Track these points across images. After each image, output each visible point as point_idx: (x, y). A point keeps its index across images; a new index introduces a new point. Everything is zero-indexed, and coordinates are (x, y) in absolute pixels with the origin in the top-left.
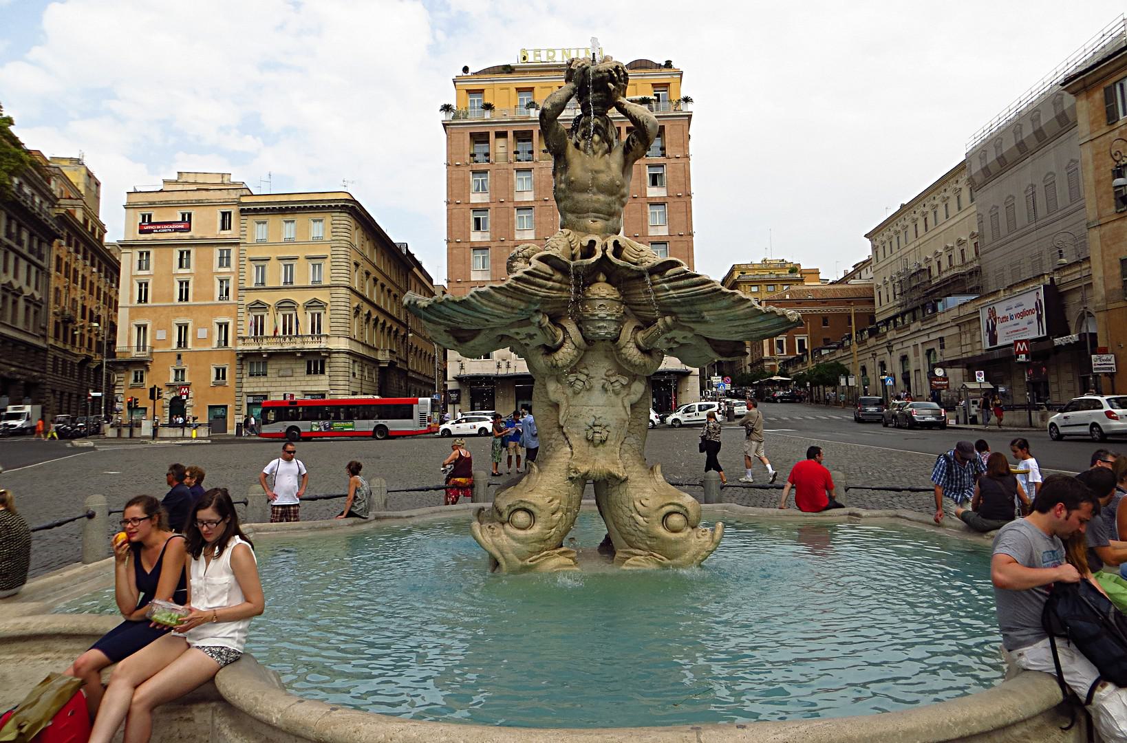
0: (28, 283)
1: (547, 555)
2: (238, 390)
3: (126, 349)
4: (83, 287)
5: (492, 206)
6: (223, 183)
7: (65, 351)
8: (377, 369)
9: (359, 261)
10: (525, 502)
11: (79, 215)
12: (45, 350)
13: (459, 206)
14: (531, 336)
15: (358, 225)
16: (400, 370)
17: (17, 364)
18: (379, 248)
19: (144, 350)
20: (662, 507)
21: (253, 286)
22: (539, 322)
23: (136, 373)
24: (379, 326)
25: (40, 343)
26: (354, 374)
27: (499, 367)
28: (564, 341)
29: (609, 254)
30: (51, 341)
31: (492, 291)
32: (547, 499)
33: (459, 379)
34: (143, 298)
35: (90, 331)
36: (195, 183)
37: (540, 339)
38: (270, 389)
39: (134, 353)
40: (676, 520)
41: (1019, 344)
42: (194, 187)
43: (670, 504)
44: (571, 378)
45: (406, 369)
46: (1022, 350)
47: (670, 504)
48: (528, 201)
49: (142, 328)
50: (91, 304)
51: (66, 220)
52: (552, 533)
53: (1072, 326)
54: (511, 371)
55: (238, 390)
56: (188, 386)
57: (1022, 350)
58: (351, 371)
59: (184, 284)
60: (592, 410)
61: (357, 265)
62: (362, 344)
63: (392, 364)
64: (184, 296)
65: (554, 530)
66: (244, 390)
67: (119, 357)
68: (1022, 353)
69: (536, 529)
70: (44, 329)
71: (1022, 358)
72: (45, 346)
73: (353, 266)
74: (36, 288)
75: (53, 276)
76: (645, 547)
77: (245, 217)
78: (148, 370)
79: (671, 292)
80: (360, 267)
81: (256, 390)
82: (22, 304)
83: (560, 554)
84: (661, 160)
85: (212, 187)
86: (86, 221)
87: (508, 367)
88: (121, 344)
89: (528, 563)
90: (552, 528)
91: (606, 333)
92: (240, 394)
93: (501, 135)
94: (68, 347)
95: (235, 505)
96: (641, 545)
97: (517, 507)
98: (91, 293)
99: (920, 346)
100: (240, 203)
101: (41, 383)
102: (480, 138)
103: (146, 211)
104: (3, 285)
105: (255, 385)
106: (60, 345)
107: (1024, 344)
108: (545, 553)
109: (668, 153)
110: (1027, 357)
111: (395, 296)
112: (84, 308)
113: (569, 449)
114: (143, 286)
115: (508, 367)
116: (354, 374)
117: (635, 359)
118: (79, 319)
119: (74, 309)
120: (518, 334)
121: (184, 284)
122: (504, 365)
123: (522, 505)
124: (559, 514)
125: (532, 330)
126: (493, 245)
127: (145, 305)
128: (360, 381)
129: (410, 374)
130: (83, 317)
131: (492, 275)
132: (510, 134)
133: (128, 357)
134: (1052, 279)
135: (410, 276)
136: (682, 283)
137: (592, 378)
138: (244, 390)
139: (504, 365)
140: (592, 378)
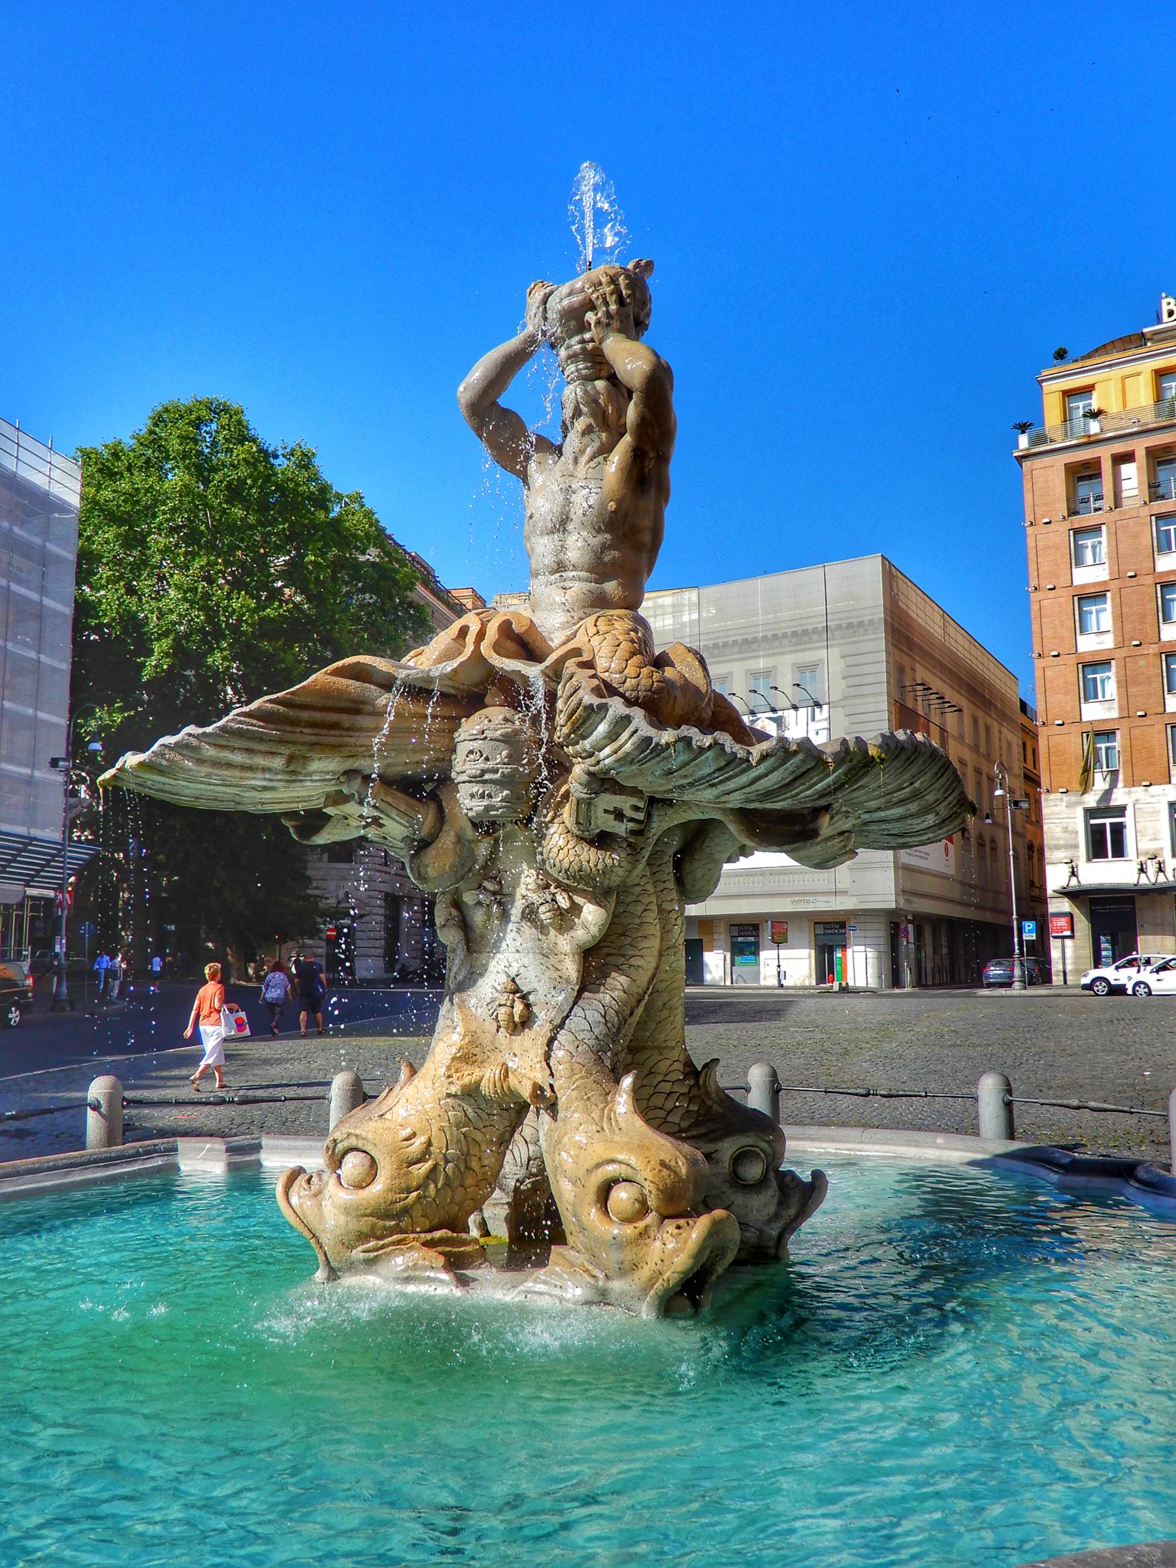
1: (399, 1242)
13: (1052, 594)
20: (598, 1165)
27: (1142, 870)
29: (486, 648)
33: (1067, 893)
40: (622, 1196)
43: (613, 1161)
47: (613, 1161)
69: (378, 1188)
83: (426, 1244)
87: (1161, 870)
90: (409, 1191)
91: (488, 808)
115: (1161, 870)
122: (1152, 867)
131: (1121, 708)
132: (1141, 454)
139: (1152, 867)
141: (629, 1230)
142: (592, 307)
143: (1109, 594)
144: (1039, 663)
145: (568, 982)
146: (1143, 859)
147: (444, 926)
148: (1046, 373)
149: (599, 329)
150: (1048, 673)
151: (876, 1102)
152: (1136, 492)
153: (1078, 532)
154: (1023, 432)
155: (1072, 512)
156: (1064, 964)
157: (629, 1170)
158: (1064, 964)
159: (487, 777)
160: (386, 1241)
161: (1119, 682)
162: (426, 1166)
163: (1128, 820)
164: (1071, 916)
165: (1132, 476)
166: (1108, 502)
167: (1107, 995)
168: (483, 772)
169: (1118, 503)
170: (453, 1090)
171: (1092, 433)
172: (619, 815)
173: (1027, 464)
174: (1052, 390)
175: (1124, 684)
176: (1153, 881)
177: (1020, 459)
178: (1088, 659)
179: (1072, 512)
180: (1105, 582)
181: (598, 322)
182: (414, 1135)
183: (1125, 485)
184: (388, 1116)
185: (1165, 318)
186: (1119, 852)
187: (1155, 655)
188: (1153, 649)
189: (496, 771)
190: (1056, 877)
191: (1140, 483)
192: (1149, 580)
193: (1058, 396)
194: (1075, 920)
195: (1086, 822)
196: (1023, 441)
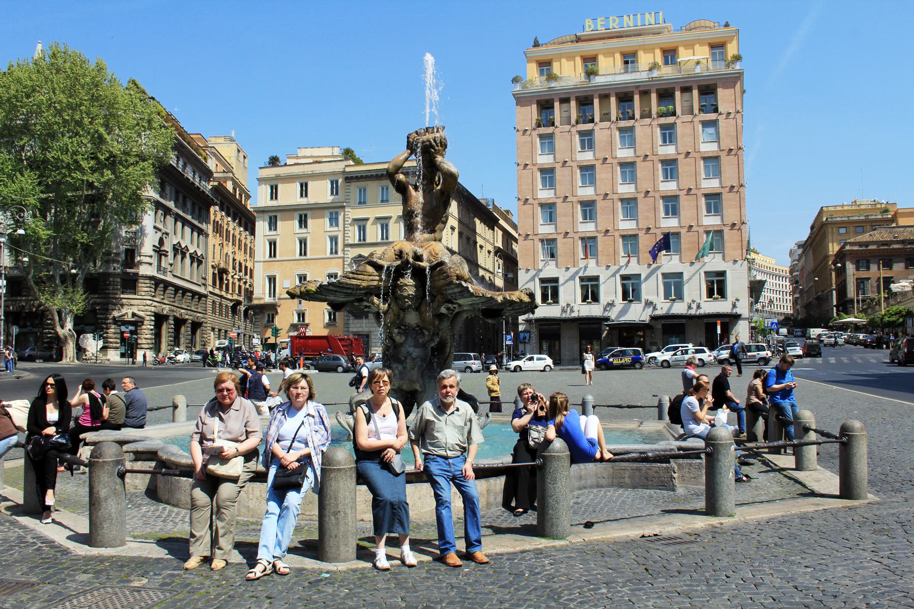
0: (192, 242)
2: (346, 329)
3: (262, 296)
4: (234, 244)
6: (333, 156)
7: (221, 297)
11: (229, 186)
12: (206, 296)
14: (369, 307)
17: (186, 307)
19: (274, 296)
21: (357, 242)
23: (269, 315)
25: (201, 290)
30: (210, 289)
34: (273, 253)
35: (240, 280)
36: (311, 157)
38: (371, 329)
39: (268, 300)
42: (311, 160)
49: (272, 280)
50: (240, 257)
51: (219, 190)
55: (346, 329)
56: (307, 325)
59: (303, 242)
64: (303, 252)
66: (351, 330)
67: (255, 302)
70: (205, 279)
72: (206, 293)
74: (198, 246)
75: (210, 236)
77: (349, 184)
78: (277, 313)
81: (360, 330)
82: (188, 260)
84: (713, 116)
85: (324, 160)
86: (235, 189)
88: (257, 293)
92: (347, 333)
94: (224, 293)
98: (240, 248)
100: (344, 172)
101: (202, 322)
102: (545, 105)
103: (274, 183)
104: (174, 245)
105: (359, 325)
106: (217, 291)
109: (720, 110)
112: (234, 260)
114: (273, 244)
115: (572, 311)
118: (231, 270)
119: (226, 262)
121: (303, 242)
127: (274, 259)
130: (234, 268)
133: (262, 302)
138: (351, 330)
155: (539, 126)
172: (448, 309)
178: (543, 201)
179: (539, 125)
185: (587, 29)
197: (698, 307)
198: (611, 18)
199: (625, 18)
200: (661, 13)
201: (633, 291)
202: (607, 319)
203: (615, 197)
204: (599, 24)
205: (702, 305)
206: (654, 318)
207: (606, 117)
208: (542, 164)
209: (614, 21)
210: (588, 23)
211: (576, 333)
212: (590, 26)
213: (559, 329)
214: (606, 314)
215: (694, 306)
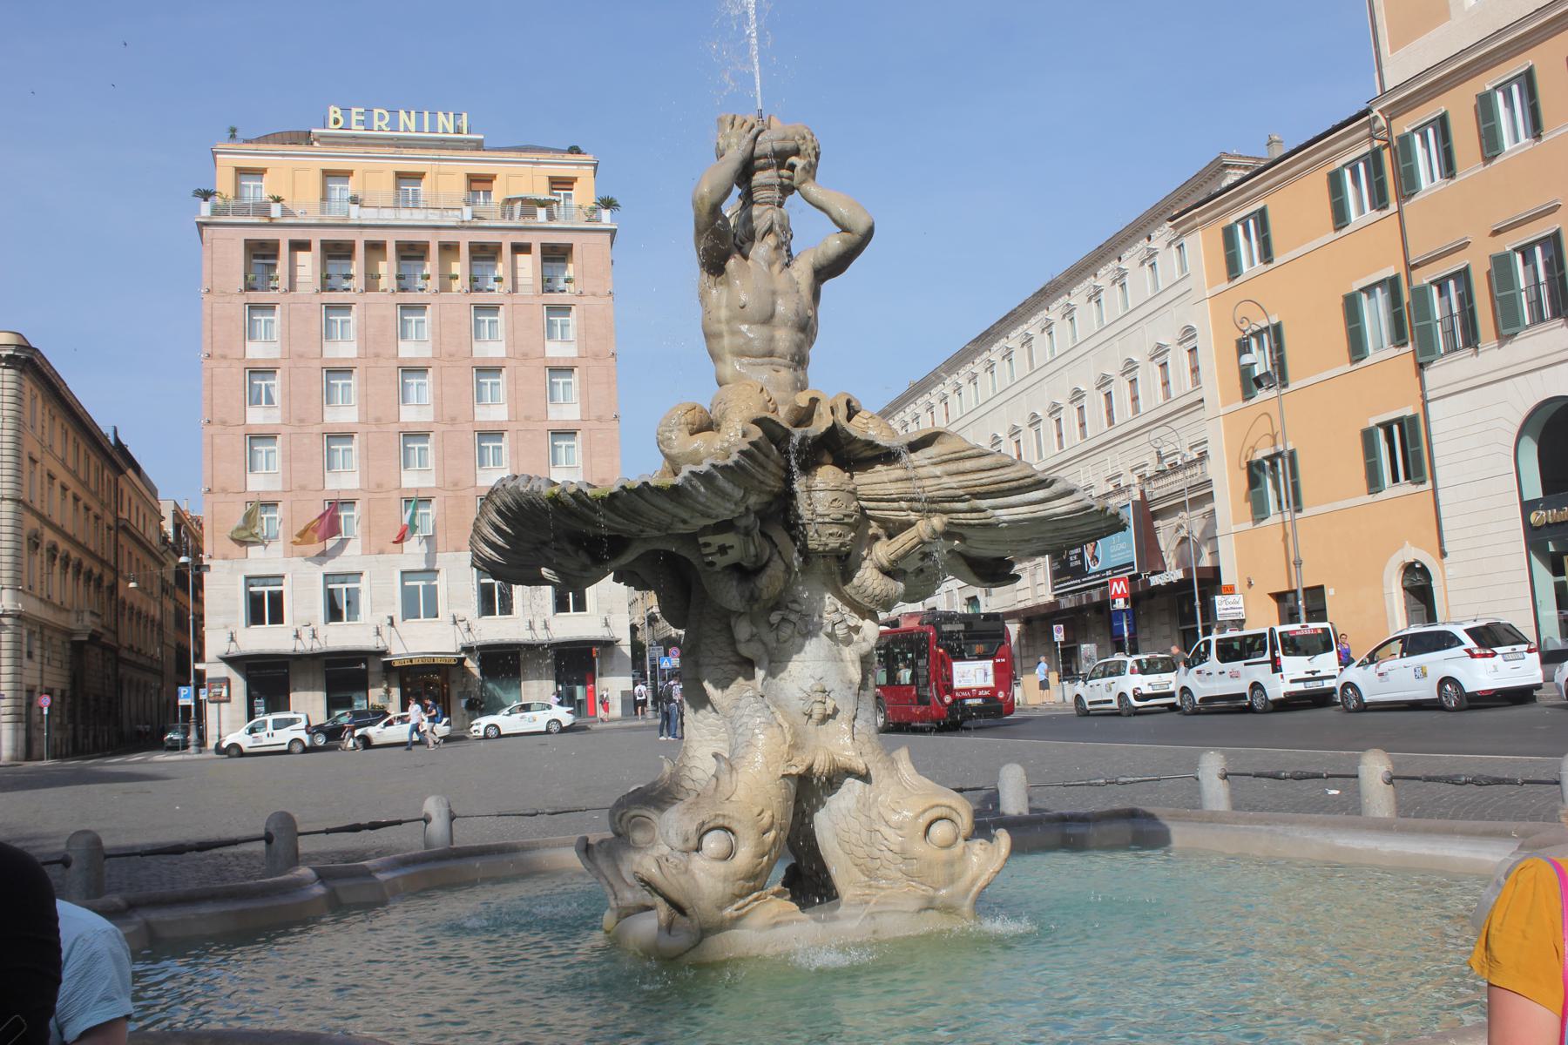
1: (756, 899)
5: (284, 364)
8: (68, 646)
9: (37, 455)
10: (724, 816)
14: (723, 550)
15: (36, 391)
16: (105, 647)
18: (71, 434)
20: (925, 811)
22: (746, 527)
24: (70, 570)
26: (30, 655)
27: (297, 636)
28: (769, 560)
31: (713, 470)
32: (757, 810)
37: (732, 557)
41: (1115, 584)
43: (937, 806)
44: (775, 618)
45: (115, 644)
46: (1119, 592)
48: (346, 359)
52: (763, 864)
53: (1170, 560)
54: (317, 646)
57: (1119, 592)
58: (25, 649)
60: (808, 667)
61: (33, 461)
62: (41, 600)
63: (94, 637)
65: (766, 858)
68: (1119, 596)
71: (1120, 604)
73: (26, 461)
76: (900, 875)
79: (945, 479)
80: (38, 465)
89: (735, 914)
91: (842, 545)
93: (299, 246)
95: (46, 868)
96: (887, 872)
97: (712, 825)
99: (956, 592)
107: (1122, 583)
108: (755, 895)
110: (1126, 603)
111: (97, 517)
113: (777, 731)
115: (314, 636)
116: (30, 655)
117: (875, 586)
120: (707, 545)
122: (306, 634)
123: (720, 822)
124: (772, 834)
125: (728, 539)
126: (285, 430)
128: (39, 666)
129: (125, 654)
132: (316, 246)
134: (1142, 492)
135: (120, 479)
136: (968, 465)
137: (806, 616)
139: (306, 634)
140: (806, 616)
141: (944, 854)
142: (797, 152)
143: (278, 371)
144: (210, 429)
145: (851, 682)
146: (299, 626)
147: (749, 641)
148: (220, 147)
149: (803, 172)
150: (217, 441)
151: (543, 819)
152: (310, 279)
153: (254, 307)
154: (206, 200)
155: (249, 287)
156: (220, 728)
157: (948, 810)
158: (220, 728)
159: (846, 520)
160: (750, 898)
161: (283, 456)
162: (772, 834)
163: (286, 589)
164: (227, 681)
165: (308, 263)
166: (283, 283)
167: (559, 732)
168: (845, 516)
169: (292, 287)
170: (794, 771)
171: (273, 216)
173: (207, 231)
174: (227, 163)
175: (289, 458)
176: (309, 647)
177: (201, 225)
179: (249, 287)
180: (275, 360)
181: (804, 168)
182: (762, 812)
183: (300, 271)
184: (733, 799)
186: (277, 618)
187: (318, 434)
188: (318, 429)
189: (851, 516)
190: (216, 642)
191: (313, 273)
192: (317, 364)
193: (232, 172)
194: (232, 684)
195: (246, 589)
196: (205, 209)
197: (546, 627)
198: (376, 112)
199: (402, 114)
200: (465, 116)
201: (348, 603)
202: (384, 653)
203: (395, 428)
204: (354, 118)
205: (552, 625)
206: (468, 650)
207: (372, 281)
208: (255, 360)
209: (381, 117)
210: (334, 112)
211: (322, 681)
212: (336, 122)
213: (287, 675)
214: (381, 646)
215: (538, 625)
